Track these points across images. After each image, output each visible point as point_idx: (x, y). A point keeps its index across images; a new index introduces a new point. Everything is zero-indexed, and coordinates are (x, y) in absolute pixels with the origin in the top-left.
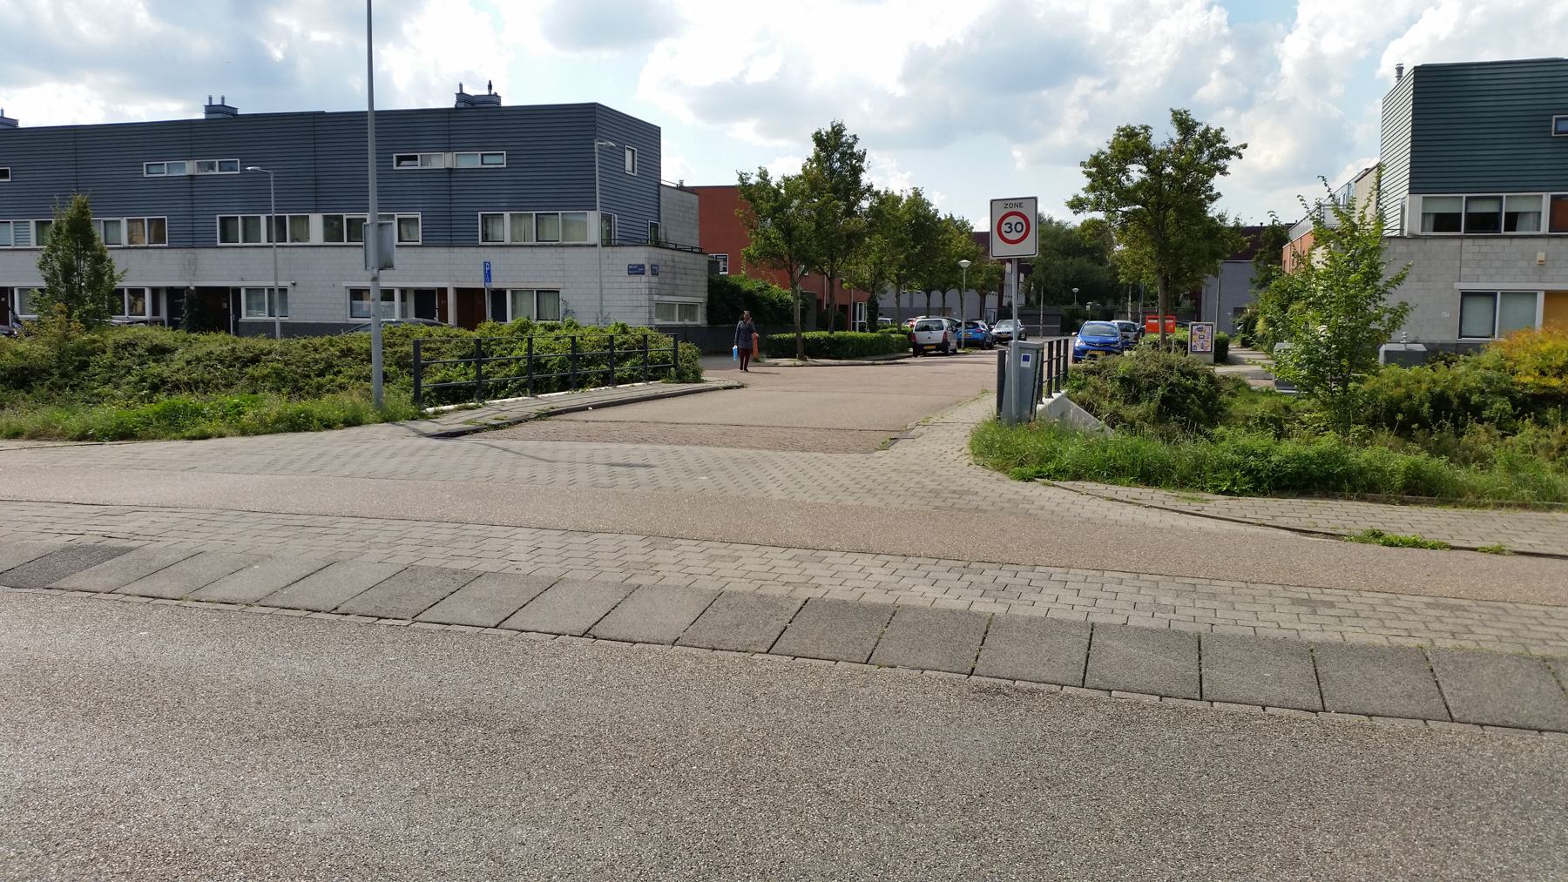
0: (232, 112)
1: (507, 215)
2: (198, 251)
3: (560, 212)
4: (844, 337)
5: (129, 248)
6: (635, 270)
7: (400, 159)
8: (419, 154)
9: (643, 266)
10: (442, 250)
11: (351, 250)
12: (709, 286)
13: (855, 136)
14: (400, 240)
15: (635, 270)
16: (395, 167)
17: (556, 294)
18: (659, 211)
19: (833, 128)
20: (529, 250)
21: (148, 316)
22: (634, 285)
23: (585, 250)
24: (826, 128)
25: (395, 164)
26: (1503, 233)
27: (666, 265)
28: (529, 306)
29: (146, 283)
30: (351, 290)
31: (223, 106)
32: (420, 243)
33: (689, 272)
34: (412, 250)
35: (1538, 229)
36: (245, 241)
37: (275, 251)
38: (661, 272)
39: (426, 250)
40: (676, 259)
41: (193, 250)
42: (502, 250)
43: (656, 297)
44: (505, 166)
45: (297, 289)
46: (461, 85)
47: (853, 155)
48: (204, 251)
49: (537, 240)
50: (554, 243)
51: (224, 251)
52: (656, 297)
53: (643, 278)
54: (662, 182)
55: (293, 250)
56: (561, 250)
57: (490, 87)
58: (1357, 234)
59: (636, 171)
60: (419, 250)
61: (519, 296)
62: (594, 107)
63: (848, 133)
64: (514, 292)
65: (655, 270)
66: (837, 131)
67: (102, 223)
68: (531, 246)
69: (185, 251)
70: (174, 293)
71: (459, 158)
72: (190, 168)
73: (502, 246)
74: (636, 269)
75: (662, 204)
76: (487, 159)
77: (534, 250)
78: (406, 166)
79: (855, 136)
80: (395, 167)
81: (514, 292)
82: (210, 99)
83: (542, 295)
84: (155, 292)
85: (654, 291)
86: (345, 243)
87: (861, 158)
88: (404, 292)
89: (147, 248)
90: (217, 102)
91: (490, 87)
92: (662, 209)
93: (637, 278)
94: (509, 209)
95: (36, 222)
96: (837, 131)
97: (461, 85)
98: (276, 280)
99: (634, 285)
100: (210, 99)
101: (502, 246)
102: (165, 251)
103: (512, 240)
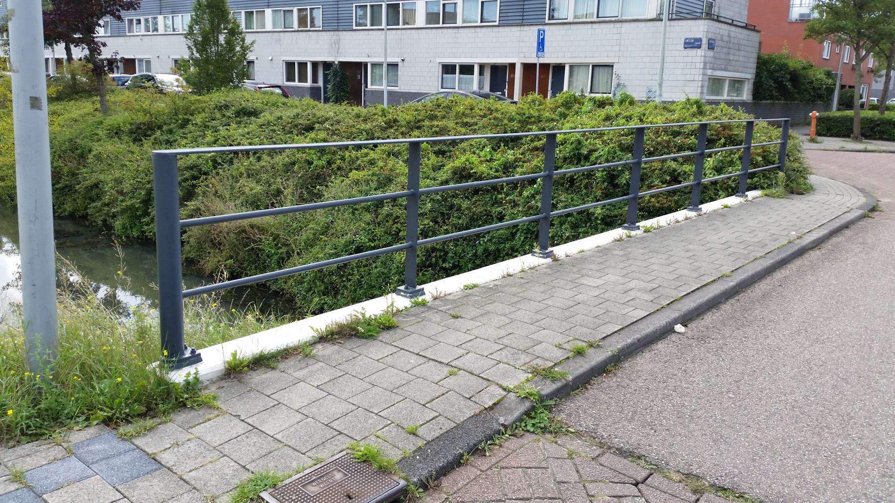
5: (298, 31)
6: (692, 44)
9: (700, 40)
10: (514, 29)
12: (758, 63)
15: (692, 44)
17: (610, 69)
20: (589, 26)
21: (309, 84)
22: (689, 59)
27: (722, 40)
29: (309, 58)
30: (443, 65)
32: (497, 23)
33: (742, 48)
34: (490, 29)
36: (372, 25)
39: (501, 29)
40: (732, 34)
43: (709, 72)
45: (405, 64)
48: (344, 33)
51: (357, 33)
52: (709, 72)
53: (700, 52)
55: (404, 31)
56: (619, 25)
60: (496, 29)
61: (575, 70)
64: (571, 67)
65: (712, 44)
67: (282, 12)
68: (592, 23)
69: (332, 33)
70: (327, 65)
73: (565, 24)
74: (693, 43)
83: (597, 69)
84: (315, 65)
85: (708, 66)
86: (441, 25)
88: (482, 67)
89: (309, 31)
93: (692, 52)
95: (246, 12)
98: (386, 57)
99: (689, 59)
101: (565, 24)
102: (320, 33)
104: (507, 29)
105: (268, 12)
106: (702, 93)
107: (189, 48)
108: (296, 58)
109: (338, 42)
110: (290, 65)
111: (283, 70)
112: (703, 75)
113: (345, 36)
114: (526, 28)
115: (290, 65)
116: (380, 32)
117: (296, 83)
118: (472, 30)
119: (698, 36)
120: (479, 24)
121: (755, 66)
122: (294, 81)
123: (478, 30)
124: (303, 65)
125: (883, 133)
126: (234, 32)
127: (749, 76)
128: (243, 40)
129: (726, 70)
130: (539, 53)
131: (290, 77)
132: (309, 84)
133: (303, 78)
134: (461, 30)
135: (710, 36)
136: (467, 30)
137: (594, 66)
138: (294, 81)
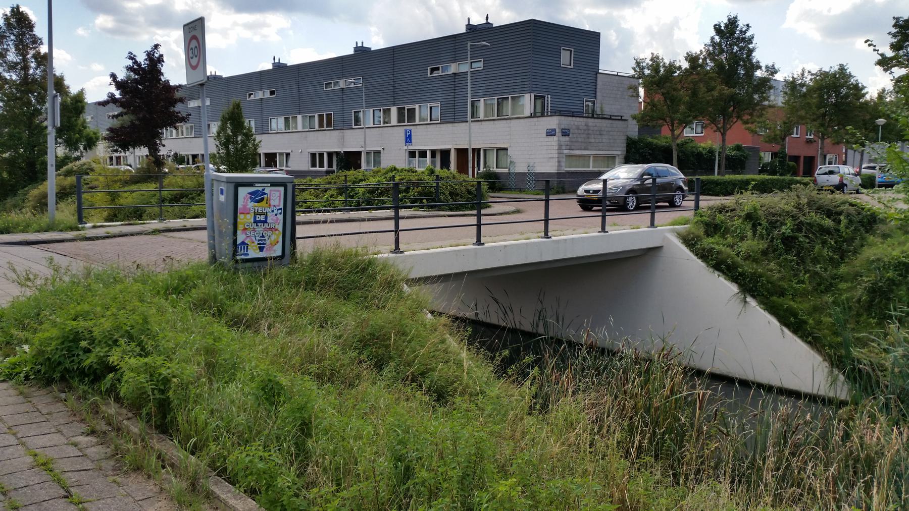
0: (368, 50)
1: (482, 100)
2: (345, 131)
3: (510, 96)
4: (707, 175)
5: (318, 130)
6: (551, 133)
7: (433, 70)
8: (440, 66)
9: (555, 130)
11: (432, 126)
12: (627, 142)
13: (748, 25)
14: (472, 117)
15: (551, 133)
16: (429, 75)
17: (505, 151)
18: (596, 91)
19: (729, 20)
20: (492, 122)
21: (325, 168)
22: (549, 144)
23: (522, 120)
24: (723, 21)
25: (429, 73)
26: (417, 122)
27: (578, 129)
28: (492, 158)
29: (326, 149)
31: (362, 47)
32: (439, 122)
33: (605, 133)
34: (435, 126)
35: (297, 129)
37: (365, 132)
38: (573, 134)
39: (442, 125)
40: (590, 124)
41: (342, 131)
42: (480, 123)
43: (566, 152)
44: (482, 68)
45: (385, 151)
46: (469, 19)
47: (744, 39)
49: (431, 120)
50: (506, 117)
52: (566, 152)
53: (555, 138)
54: (600, 71)
55: (383, 128)
56: (509, 121)
57: (487, 18)
58: (756, 97)
59: (572, 64)
60: (438, 125)
61: (487, 152)
62: (532, 23)
63: (741, 23)
64: (485, 150)
66: (732, 23)
68: (493, 120)
69: (339, 131)
70: (338, 153)
71: (460, 65)
72: (342, 84)
73: (478, 121)
74: (551, 132)
75: (599, 87)
76: (474, 65)
77: (496, 122)
78: (436, 74)
79: (748, 25)
80: (429, 75)
81: (485, 150)
82: (357, 43)
83: (499, 151)
84: (330, 155)
85: (564, 147)
86: (406, 124)
87: (750, 40)
88: (433, 153)
89: (325, 130)
90: (360, 45)
91: (487, 18)
92: (598, 90)
93: (551, 138)
94: (483, 96)
96: (732, 23)
97: (469, 19)
98: (365, 147)
99: (549, 144)
100: (357, 43)
101: (478, 121)
102: (332, 131)
103: (485, 116)
104: (445, 125)
105: (299, 117)
106: (559, 166)
107: (217, 146)
108: (317, 150)
109: (343, 138)
110: (313, 155)
111: (308, 159)
112: (559, 153)
113: (348, 133)
114: (456, 124)
115: (313, 155)
116: (361, 130)
117: (317, 168)
118: (425, 126)
119: (554, 127)
120: (429, 122)
121: (625, 145)
122: (316, 167)
123: (428, 126)
124: (321, 155)
125: (710, 190)
126: (248, 136)
127: (619, 153)
128: (254, 140)
129: (585, 149)
130: (407, 144)
131: (314, 165)
132: (325, 168)
133: (322, 165)
134: (418, 127)
135: (563, 127)
136: (421, 126)
137: (498, 150)
138: (316, 167)
